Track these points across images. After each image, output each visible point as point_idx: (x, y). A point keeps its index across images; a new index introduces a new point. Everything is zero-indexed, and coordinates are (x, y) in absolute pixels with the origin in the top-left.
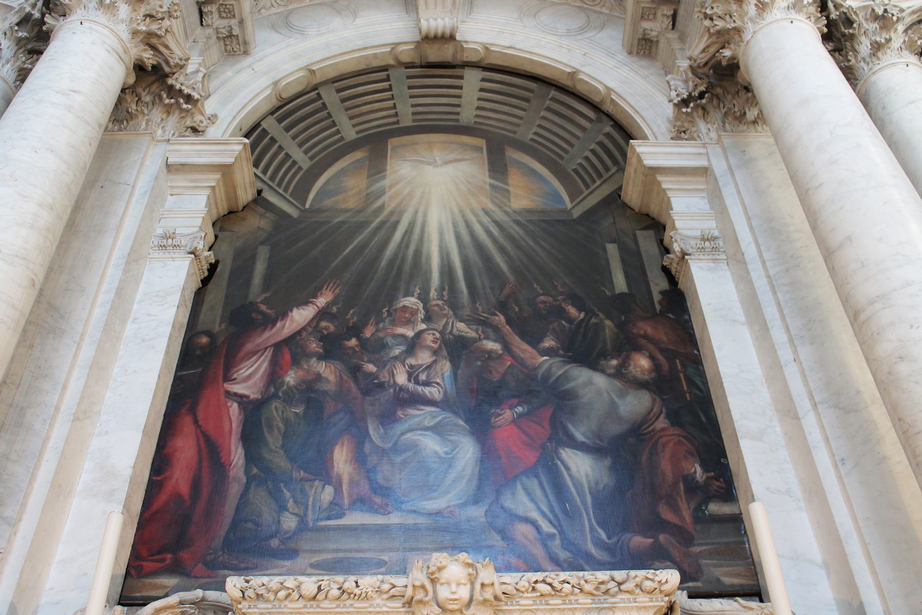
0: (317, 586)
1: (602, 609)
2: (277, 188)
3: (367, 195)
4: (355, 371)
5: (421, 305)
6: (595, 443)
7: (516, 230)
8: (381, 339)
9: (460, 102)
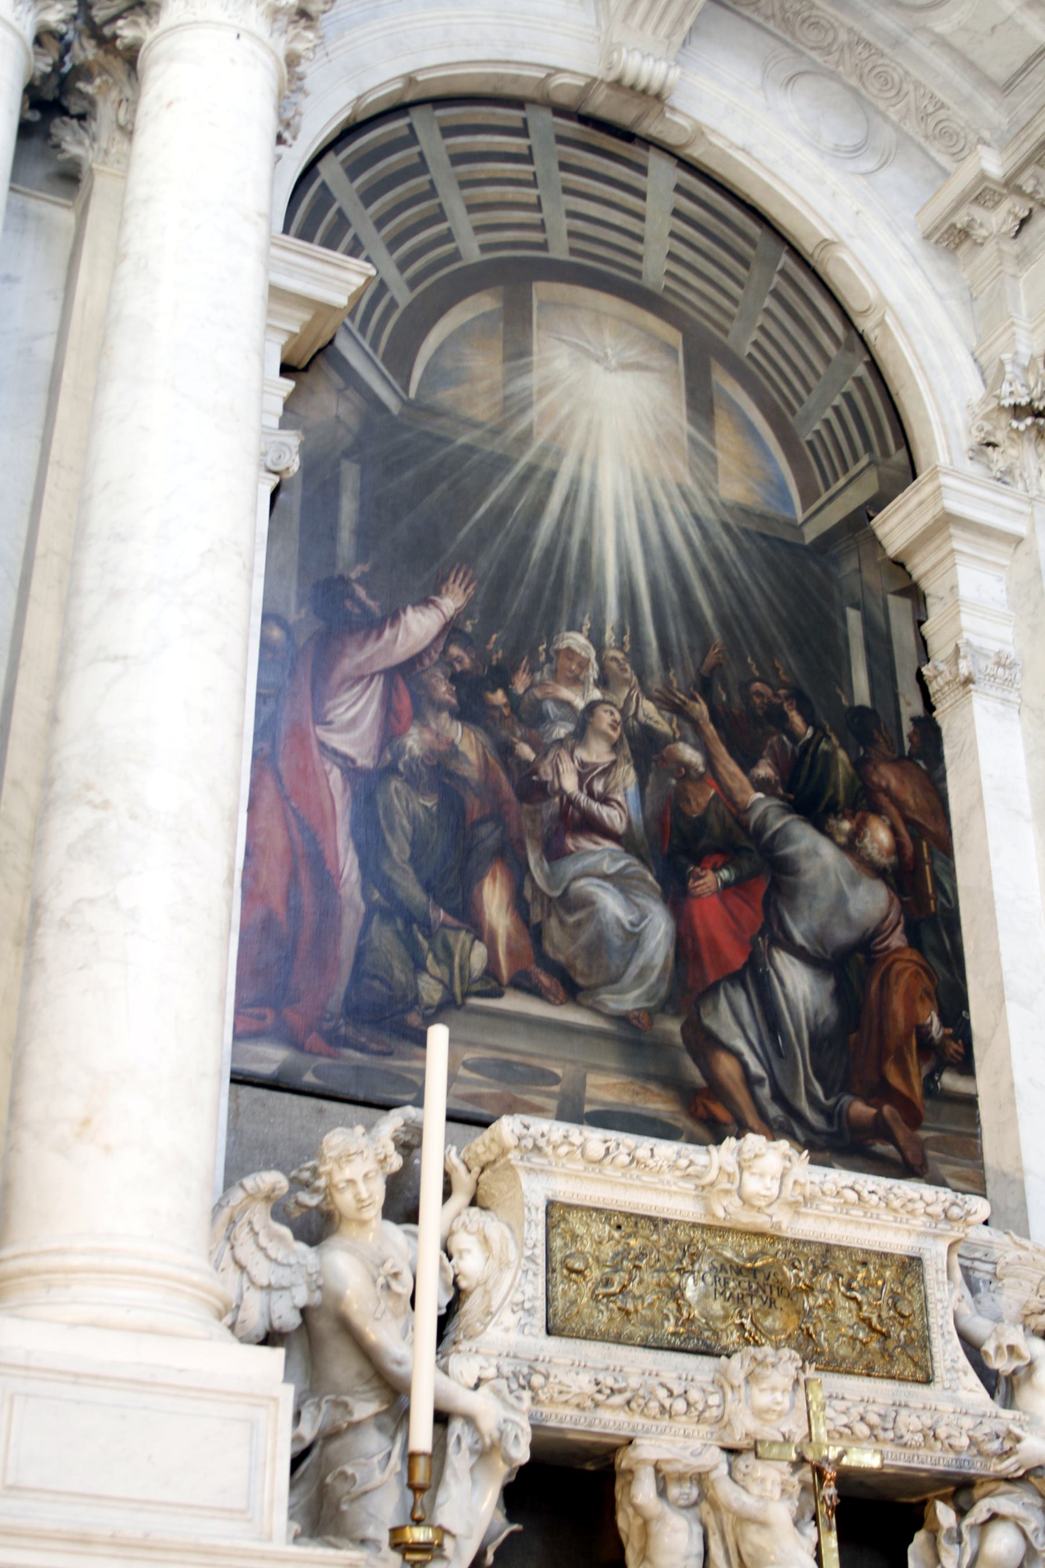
1: (899, 1229)
3: (506, 398)
4: (506, 751)
5: (592, 654)
6: (816, 951)
7: (724, 543)
8: (539, 702)
9: (643, 230)
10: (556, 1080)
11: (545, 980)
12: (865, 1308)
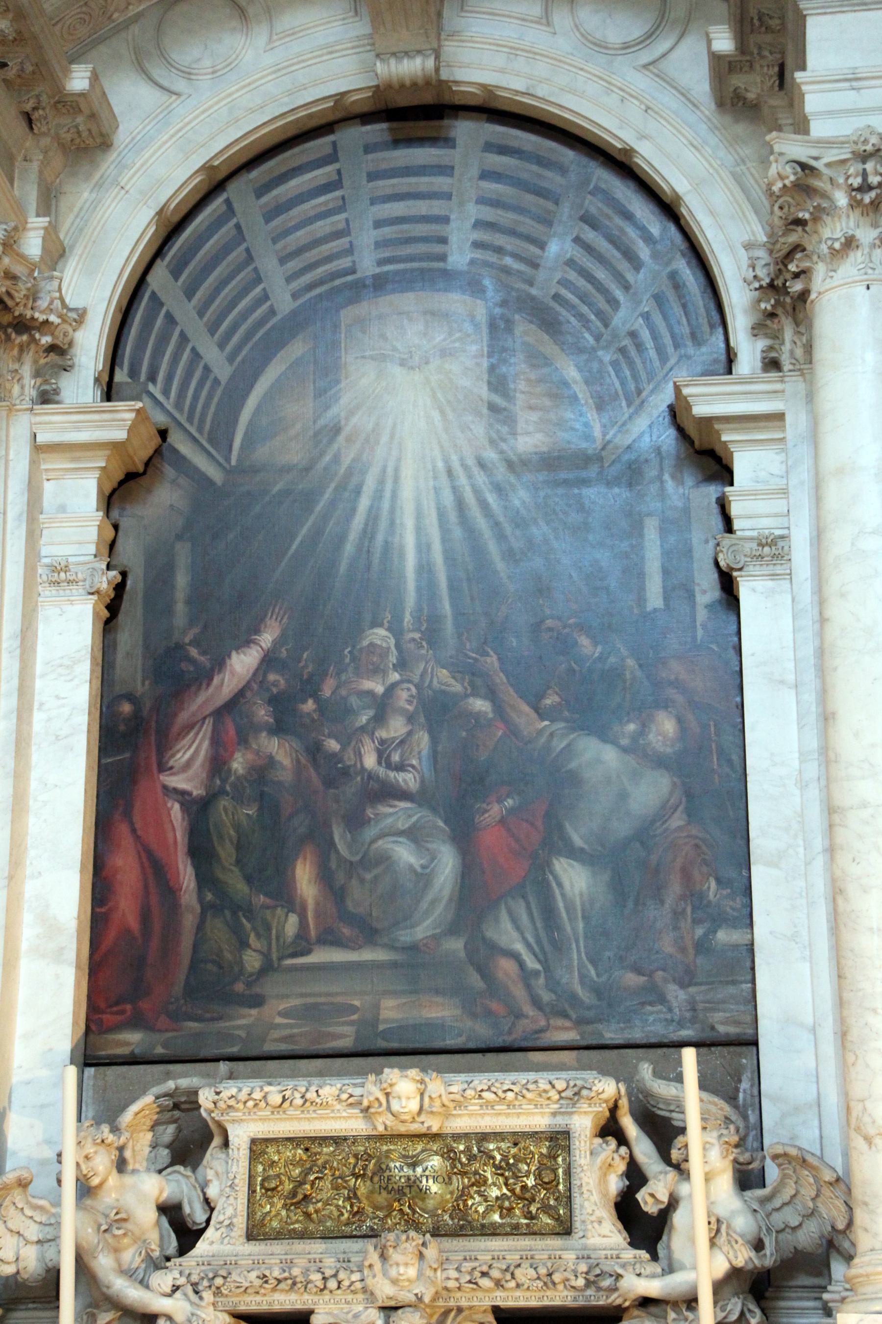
0: (281, 1095)
2: (187, 425)
5: (392, 642)
8: (345, 699)
10: (354, 1009)
11: (346, 931)
12: (511, 1181)
